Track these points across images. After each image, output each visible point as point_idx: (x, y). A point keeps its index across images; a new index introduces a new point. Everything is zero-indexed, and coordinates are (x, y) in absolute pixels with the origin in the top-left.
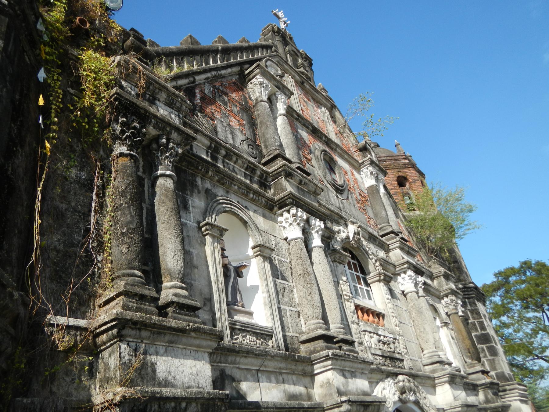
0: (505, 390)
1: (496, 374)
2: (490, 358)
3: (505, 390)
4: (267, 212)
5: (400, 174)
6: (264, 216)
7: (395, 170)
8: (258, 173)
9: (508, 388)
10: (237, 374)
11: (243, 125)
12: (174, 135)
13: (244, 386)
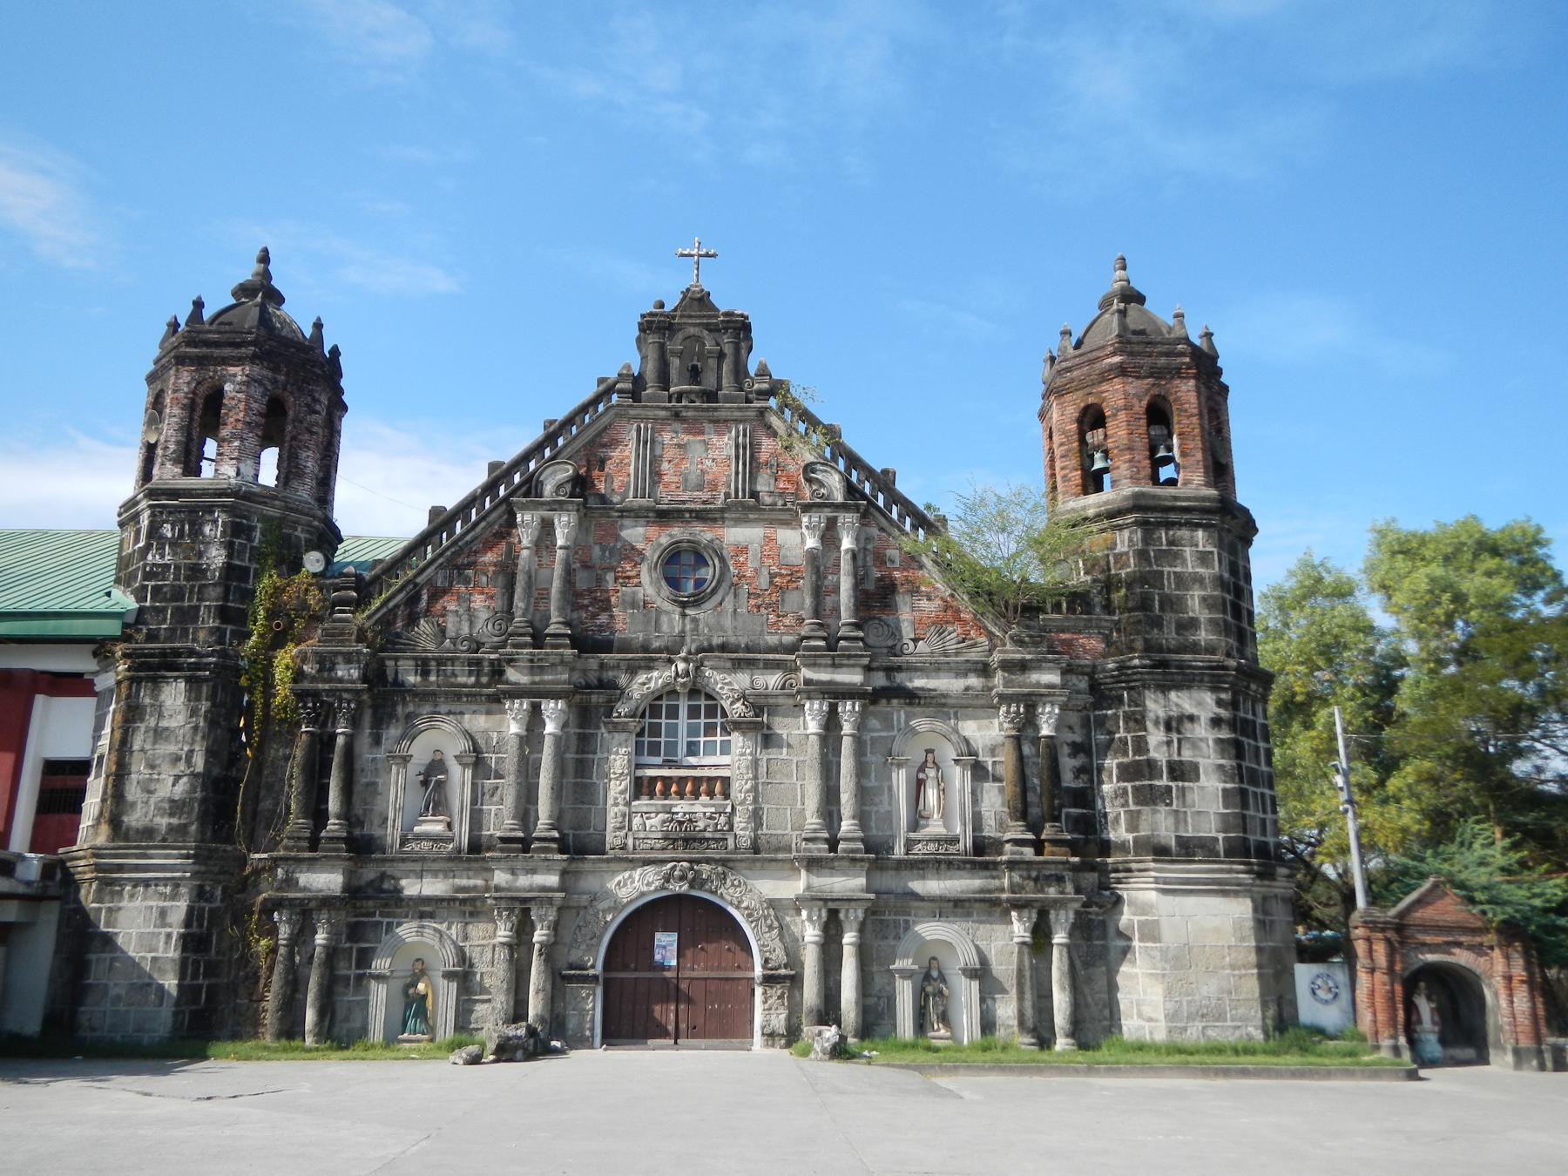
0: (1130, 870)
1: (1136, 840)
2: (1132, 807)
3: (1130, 870)
4: (495, 706)
5: (1091, 400)
6: (488, 713)
7: (1080, 393)
8: (486, 664)
9: (1134, 866)
10: (397, 874)
11: (492, 597)
12: (345, 695)
13: (403, 882)
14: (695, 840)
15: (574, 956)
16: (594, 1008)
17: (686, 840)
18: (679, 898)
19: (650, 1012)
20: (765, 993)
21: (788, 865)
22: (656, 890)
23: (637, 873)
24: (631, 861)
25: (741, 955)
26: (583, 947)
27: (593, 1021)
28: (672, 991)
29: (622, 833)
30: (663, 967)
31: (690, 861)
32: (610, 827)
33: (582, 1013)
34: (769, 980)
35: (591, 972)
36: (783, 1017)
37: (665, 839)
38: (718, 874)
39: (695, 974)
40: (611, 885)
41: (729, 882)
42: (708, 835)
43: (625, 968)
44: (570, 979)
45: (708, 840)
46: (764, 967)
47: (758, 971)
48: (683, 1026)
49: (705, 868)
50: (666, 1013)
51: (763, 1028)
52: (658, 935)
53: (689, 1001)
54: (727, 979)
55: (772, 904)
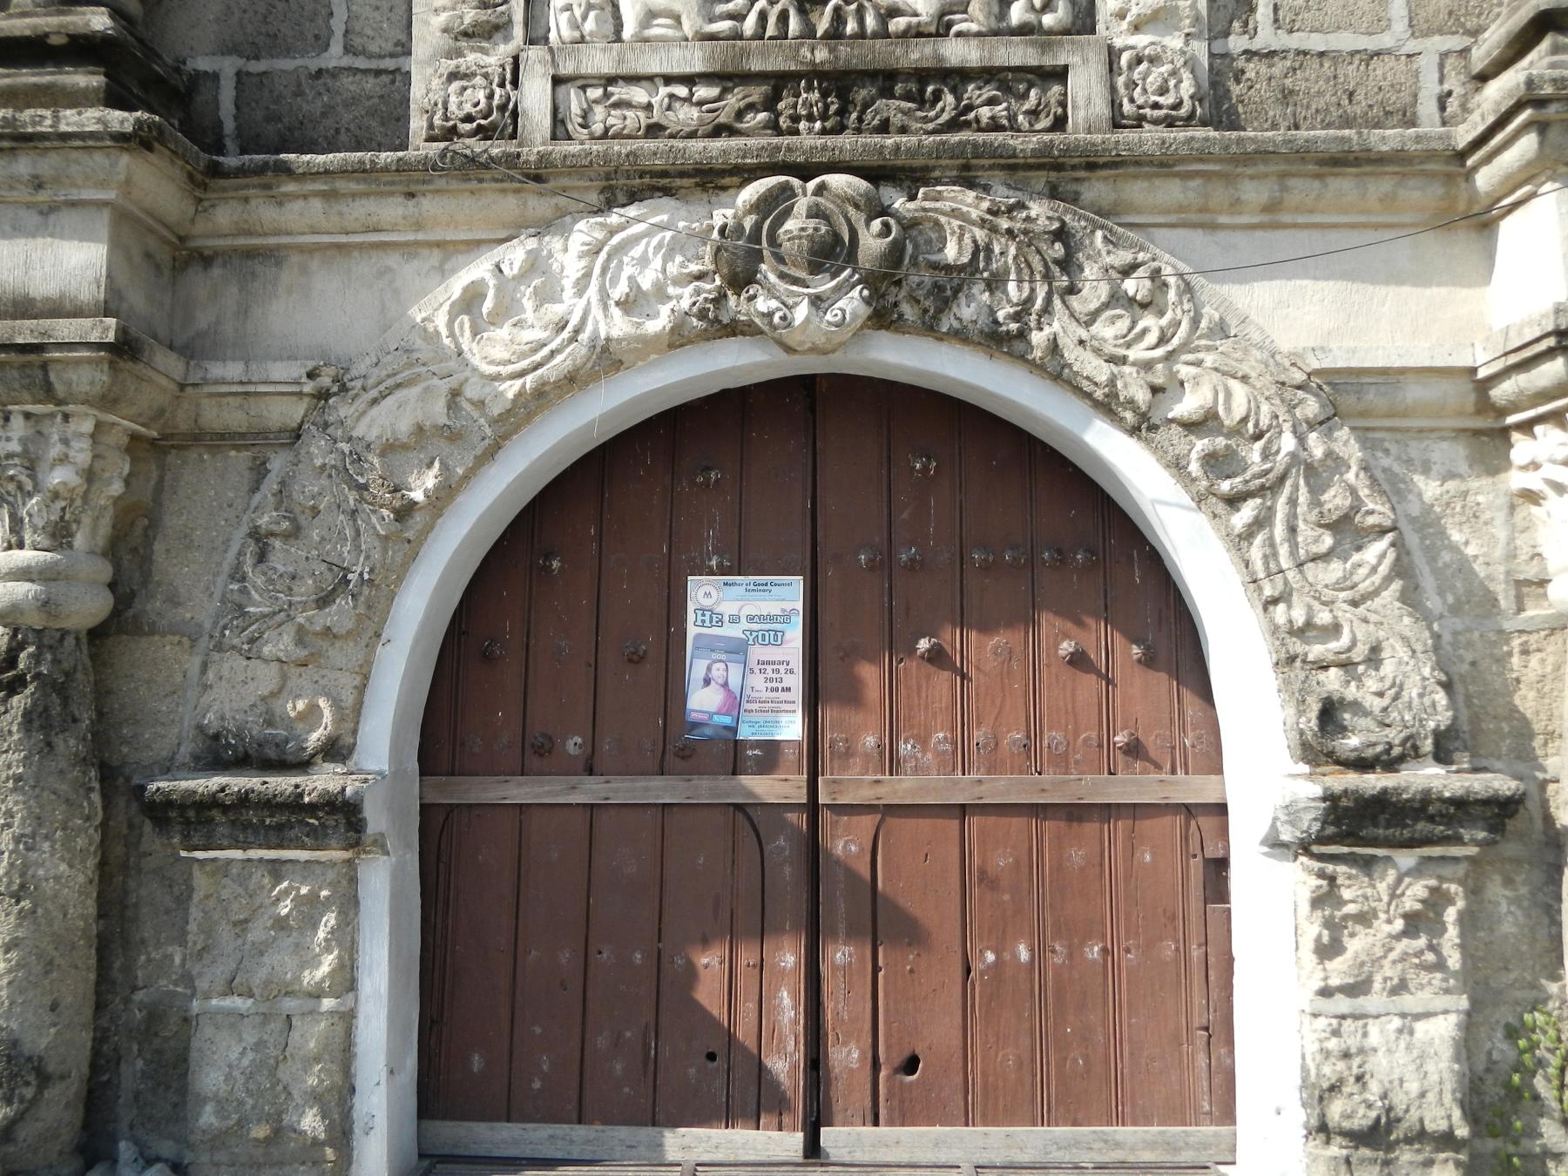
14: (886, 79)
15: (232, 693)
16: (347, 980)
17: (839, 84)
18: (806, 406)
19: (669, 985)
20: (1326, 898)
21: (1420, 195)
22: (678, 339)
23: (570, 250)
24: (538, 175)
25: (1144, 694)
26: (280, 644)
27: (344, 1052)
28: (788, 874)
29: (495, 57)
30: (734, 755)
31: (876, 174)
32: (428, 31)
33: (278, 1006)
34: (1355, 827)
35: (323, 781)
36: (1441, 1030)
37: (725, 79)
38: (1027, 238)
39: (903, 788)
40: (433, 308)
41: (1093, 292)
42: (956, 52)
43: (536, 755)
44: (200, 819)
45: (958, 77)
46: (1317, 751)
47: (1263, 777)
48: (846, 1056)
49: (957, 217)
50: (755, 989)
51: (1322, 1094)
52: (703, 592)
53: (881, 922)
54: (1076, 813)
55: (1344, 394)
